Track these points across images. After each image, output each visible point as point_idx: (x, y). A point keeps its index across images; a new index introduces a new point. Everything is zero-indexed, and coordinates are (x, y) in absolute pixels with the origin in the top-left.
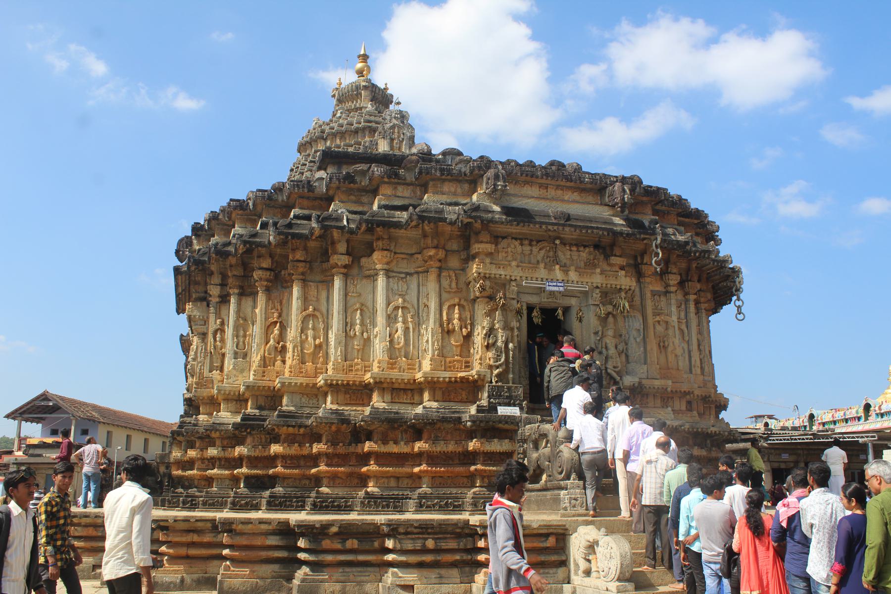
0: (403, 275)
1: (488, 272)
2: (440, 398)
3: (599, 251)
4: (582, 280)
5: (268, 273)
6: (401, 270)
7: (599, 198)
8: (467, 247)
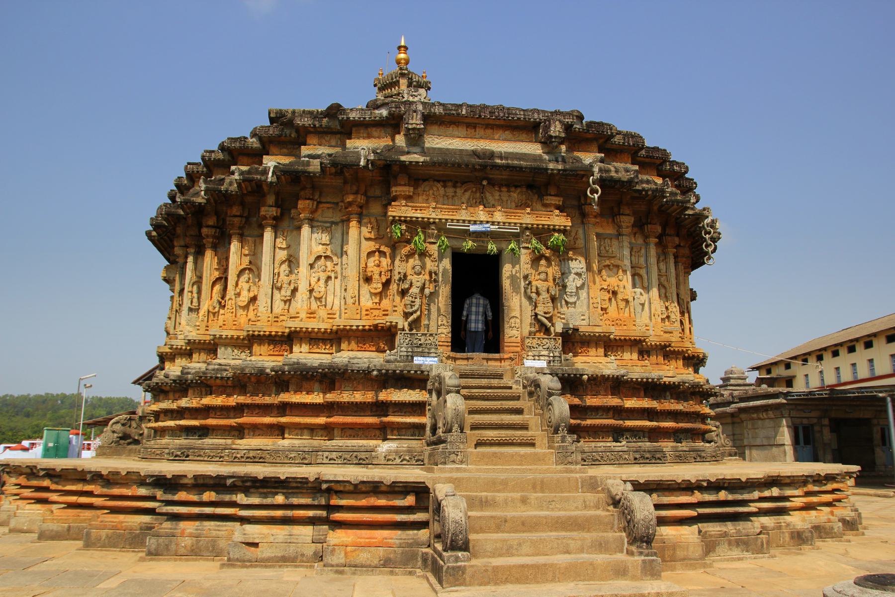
1: (402, 215)
3: (532, 192)
4: (509, 221)
5: (213, 230)
6: (326, 219)
7: (534, 135)
8: (388, 192)
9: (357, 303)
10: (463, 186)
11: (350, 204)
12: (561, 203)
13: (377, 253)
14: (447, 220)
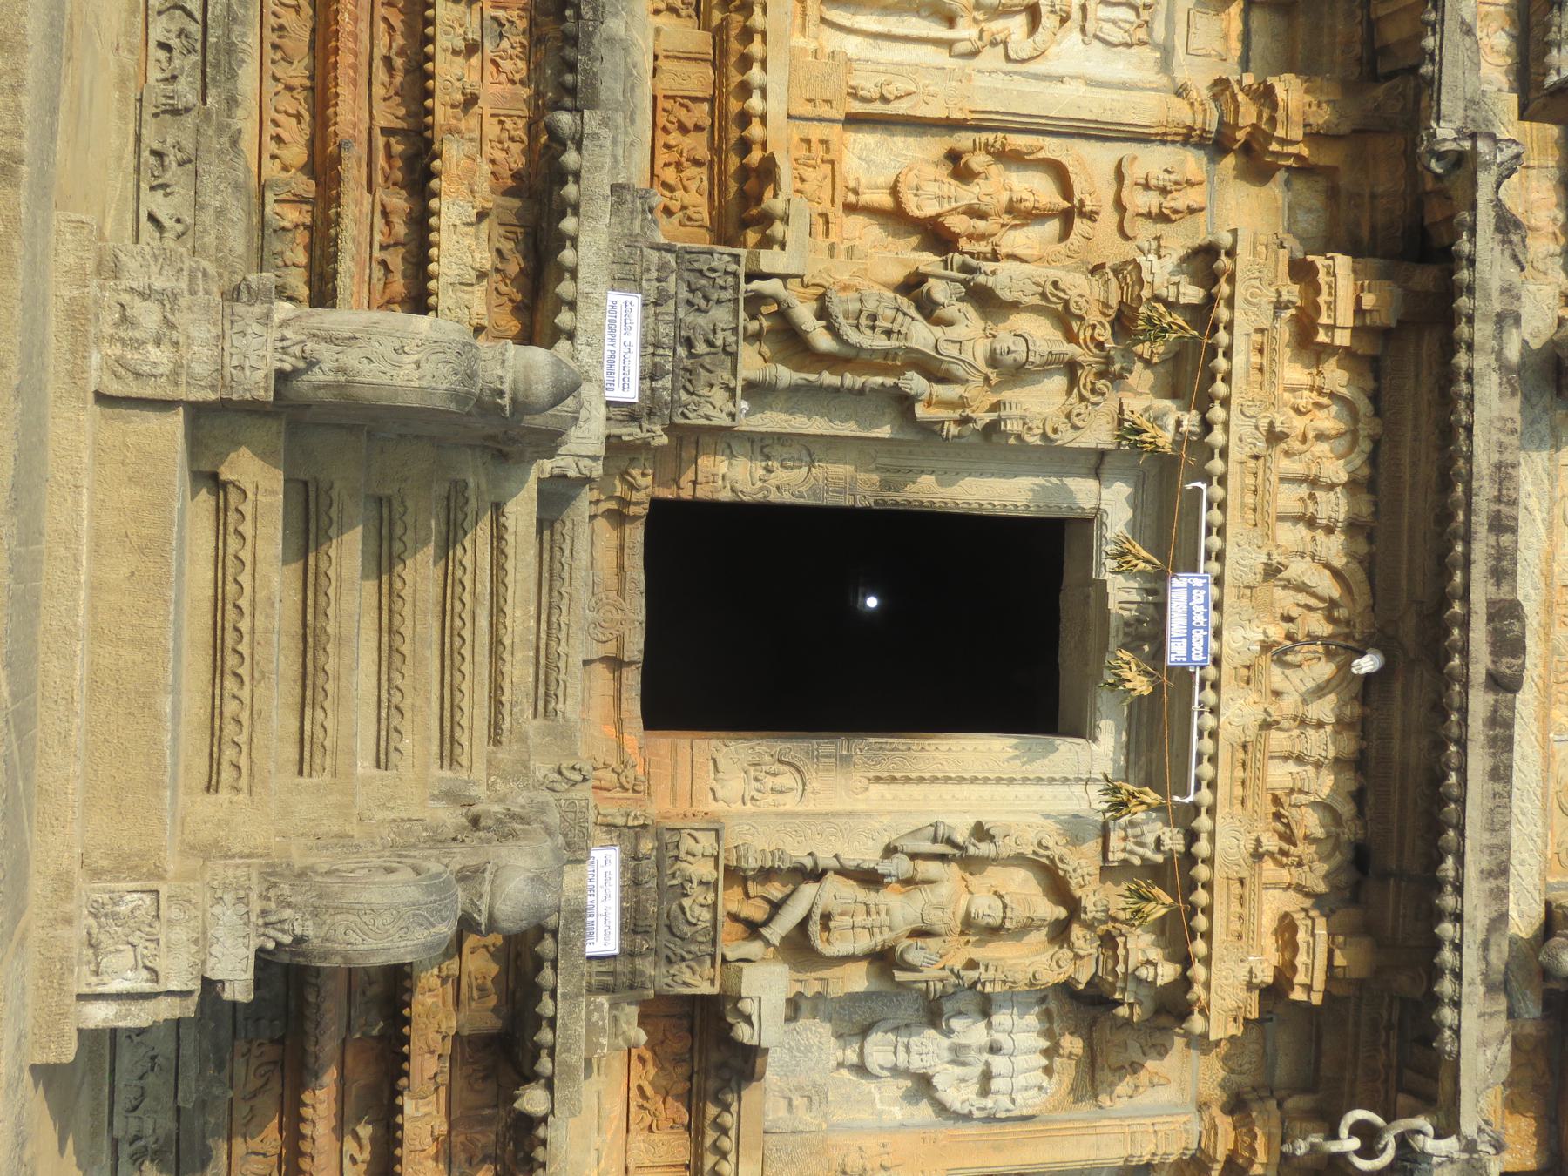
0: (1159, 33)
2: (668, 84)
4: (1224, 757)
6: (1181, 28)
9: (857, 107)
10: (1354, 566)
11: (1265, 96)
12: (1298, 995)
13: (1066, 204)
14: (1222, 481)
